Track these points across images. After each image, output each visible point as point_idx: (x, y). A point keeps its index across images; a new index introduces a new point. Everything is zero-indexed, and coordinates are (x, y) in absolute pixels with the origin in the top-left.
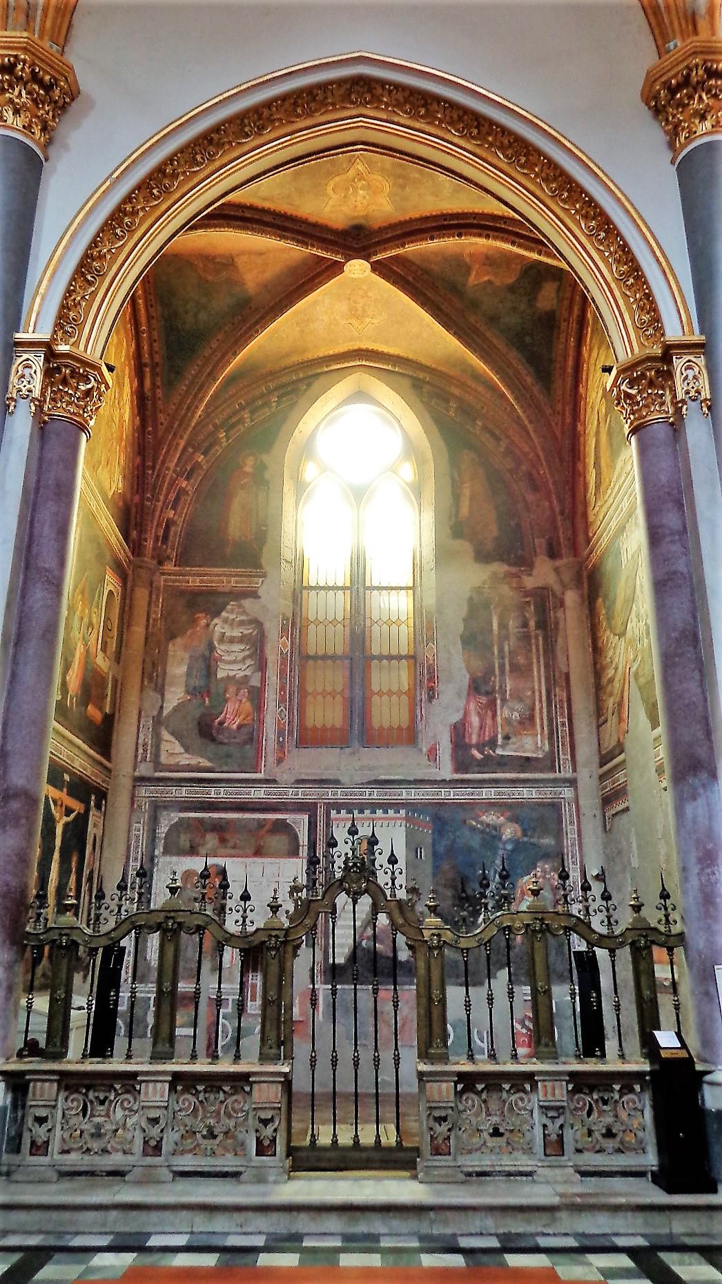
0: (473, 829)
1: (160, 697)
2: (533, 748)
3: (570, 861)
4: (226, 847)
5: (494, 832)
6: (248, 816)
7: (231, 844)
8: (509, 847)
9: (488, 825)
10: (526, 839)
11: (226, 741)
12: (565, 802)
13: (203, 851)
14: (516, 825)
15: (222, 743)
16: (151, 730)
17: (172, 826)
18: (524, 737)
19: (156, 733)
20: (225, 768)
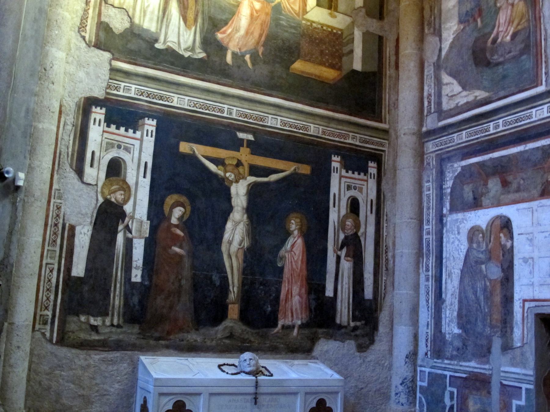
1: (438, 39)
4: (509, 192)
6: (531, 145)
7: (514, 186)
11: (501, 59)
13: (485, 201)
15: (498, 64)
16: (433, 79)
17: (456, 177)
19: (437, 79)
20: (502, 93)
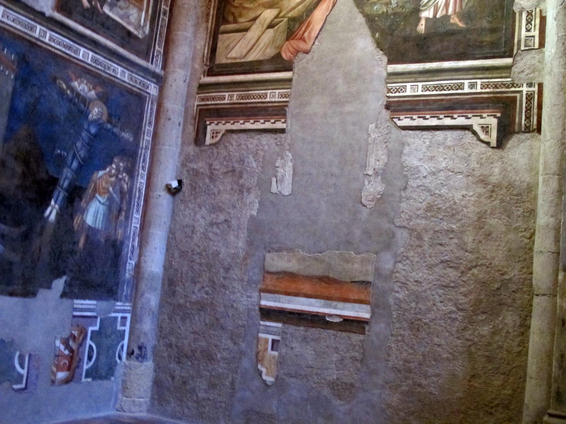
0: (61, 93)
2: (136, 23)
3: (141, 164)
5: (82, 106)
8: (93, 130)
9: (78, 95)
10: (109, 126)
12: (149, 98)
14: (105, 108)
18: (131, 6)
